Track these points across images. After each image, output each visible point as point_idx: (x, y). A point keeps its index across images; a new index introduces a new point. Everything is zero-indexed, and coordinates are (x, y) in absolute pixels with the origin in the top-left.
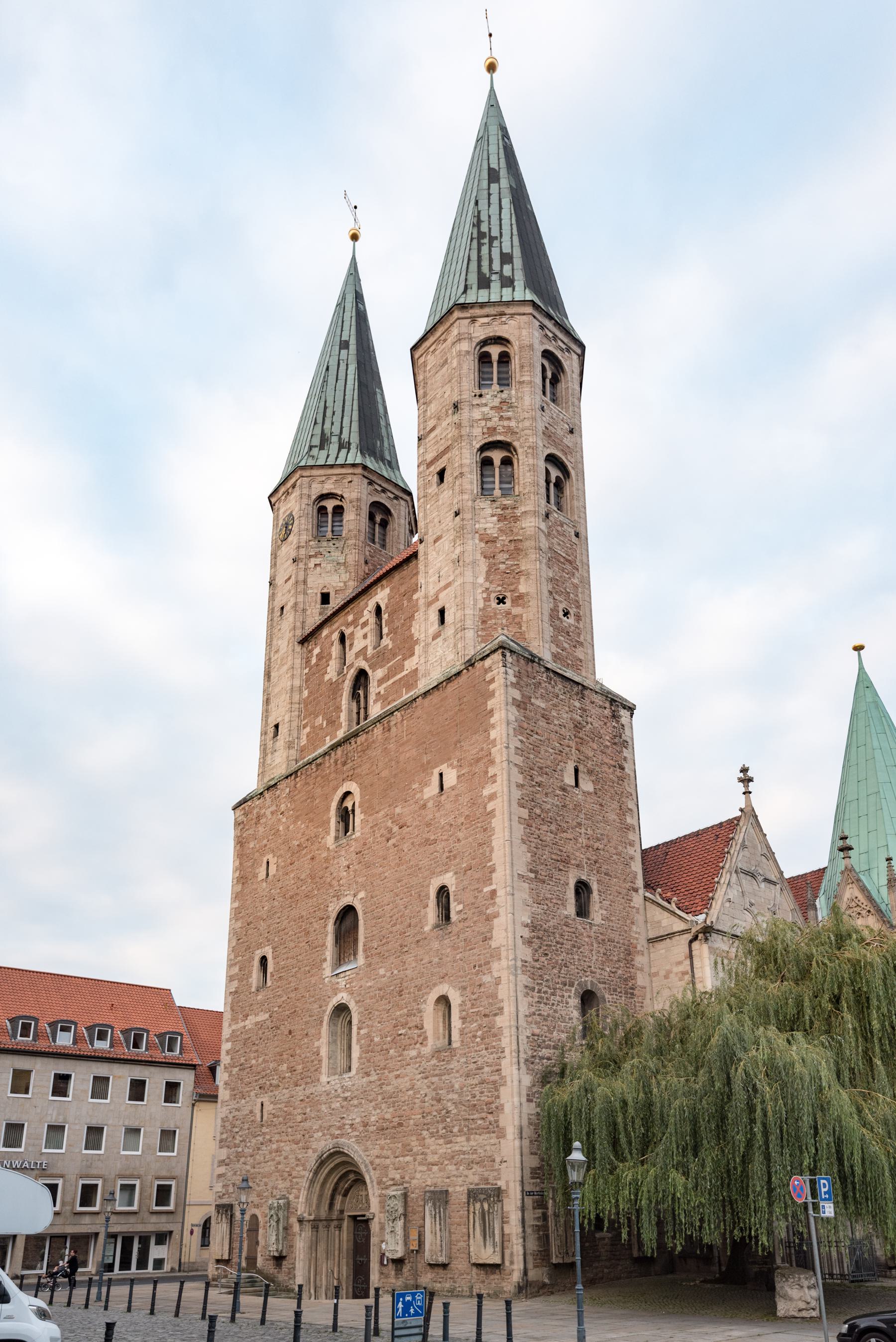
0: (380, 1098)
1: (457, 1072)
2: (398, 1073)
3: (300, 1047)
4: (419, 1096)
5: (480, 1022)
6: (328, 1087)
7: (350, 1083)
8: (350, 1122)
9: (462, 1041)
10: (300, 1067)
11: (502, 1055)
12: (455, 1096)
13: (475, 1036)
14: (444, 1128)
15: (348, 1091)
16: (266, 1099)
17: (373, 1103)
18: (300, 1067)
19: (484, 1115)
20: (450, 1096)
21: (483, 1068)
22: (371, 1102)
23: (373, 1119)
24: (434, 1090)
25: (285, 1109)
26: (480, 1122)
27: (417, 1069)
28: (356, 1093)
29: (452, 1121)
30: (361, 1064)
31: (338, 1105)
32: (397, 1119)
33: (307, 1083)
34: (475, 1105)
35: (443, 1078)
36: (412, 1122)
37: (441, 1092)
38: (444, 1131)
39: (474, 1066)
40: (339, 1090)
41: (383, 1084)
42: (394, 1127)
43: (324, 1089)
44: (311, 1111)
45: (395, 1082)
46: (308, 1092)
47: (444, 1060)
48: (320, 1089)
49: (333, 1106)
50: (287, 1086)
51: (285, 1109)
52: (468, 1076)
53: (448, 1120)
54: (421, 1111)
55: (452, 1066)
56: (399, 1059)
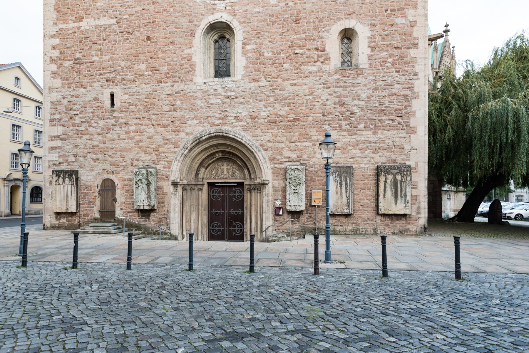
0: (272, 99)
1: (365, 86)
2: (295, 82)
3: (164, 52)
4: (320, 100)
5: (391, 52)
6: (204, 87)
7: (234, 86)
8: (235, 115)
9: (371, 64)
10: (166, 68)
11: (416, 77)
12: (362, 103)
13: (385, 62)
14: (348, 124)
15: (230, 91)
16: (118, 91)
17: (264, 103)
18: (166, 68)
19: (392, 117)
20: (356, 102)
21: (393, 85)
22: (261, 101)
23: (263, 114)
24: (337, 97)
25: (147, 100)
26: (387, 122)
27: (317, 81)
28: (241, 94)
29: (356, 120)
30: (247, 72)
31: (219, 101)
32: (293, 116)
33: (174, 82)
34: (383, 110)
35: (348, 89)
36: (311, 118)
37: (346, 99)
38: (348, 126)
39: (384, 83)
40: (220, 90)
41: (276, 89)
42: (290, 121)
43: (199, 88)
44: (182, 103)
45: (291, 89)
46: (177, 88)
47: (349, 76)
48: (192, 87)
49: (211, 101)
50: (147, 81)
51: (147, 100)
52: (375, 89)
53: (353, 119)
54: (321, 111)
55: (359, 81)
56: (296, 71)
